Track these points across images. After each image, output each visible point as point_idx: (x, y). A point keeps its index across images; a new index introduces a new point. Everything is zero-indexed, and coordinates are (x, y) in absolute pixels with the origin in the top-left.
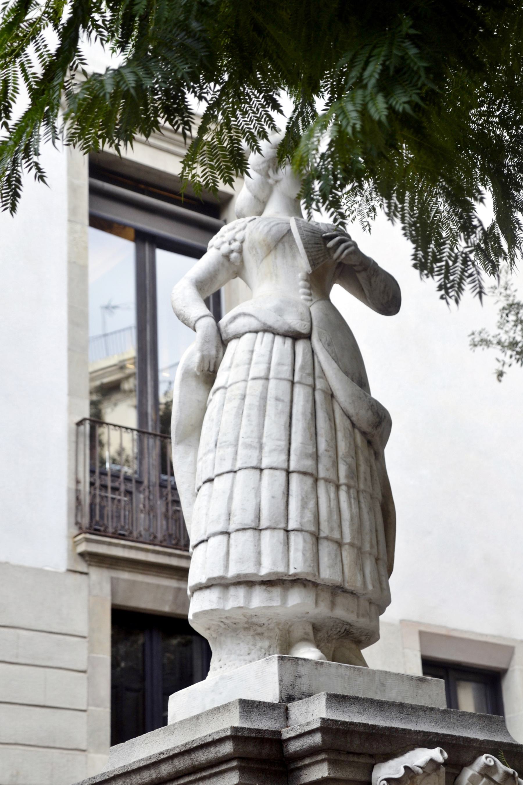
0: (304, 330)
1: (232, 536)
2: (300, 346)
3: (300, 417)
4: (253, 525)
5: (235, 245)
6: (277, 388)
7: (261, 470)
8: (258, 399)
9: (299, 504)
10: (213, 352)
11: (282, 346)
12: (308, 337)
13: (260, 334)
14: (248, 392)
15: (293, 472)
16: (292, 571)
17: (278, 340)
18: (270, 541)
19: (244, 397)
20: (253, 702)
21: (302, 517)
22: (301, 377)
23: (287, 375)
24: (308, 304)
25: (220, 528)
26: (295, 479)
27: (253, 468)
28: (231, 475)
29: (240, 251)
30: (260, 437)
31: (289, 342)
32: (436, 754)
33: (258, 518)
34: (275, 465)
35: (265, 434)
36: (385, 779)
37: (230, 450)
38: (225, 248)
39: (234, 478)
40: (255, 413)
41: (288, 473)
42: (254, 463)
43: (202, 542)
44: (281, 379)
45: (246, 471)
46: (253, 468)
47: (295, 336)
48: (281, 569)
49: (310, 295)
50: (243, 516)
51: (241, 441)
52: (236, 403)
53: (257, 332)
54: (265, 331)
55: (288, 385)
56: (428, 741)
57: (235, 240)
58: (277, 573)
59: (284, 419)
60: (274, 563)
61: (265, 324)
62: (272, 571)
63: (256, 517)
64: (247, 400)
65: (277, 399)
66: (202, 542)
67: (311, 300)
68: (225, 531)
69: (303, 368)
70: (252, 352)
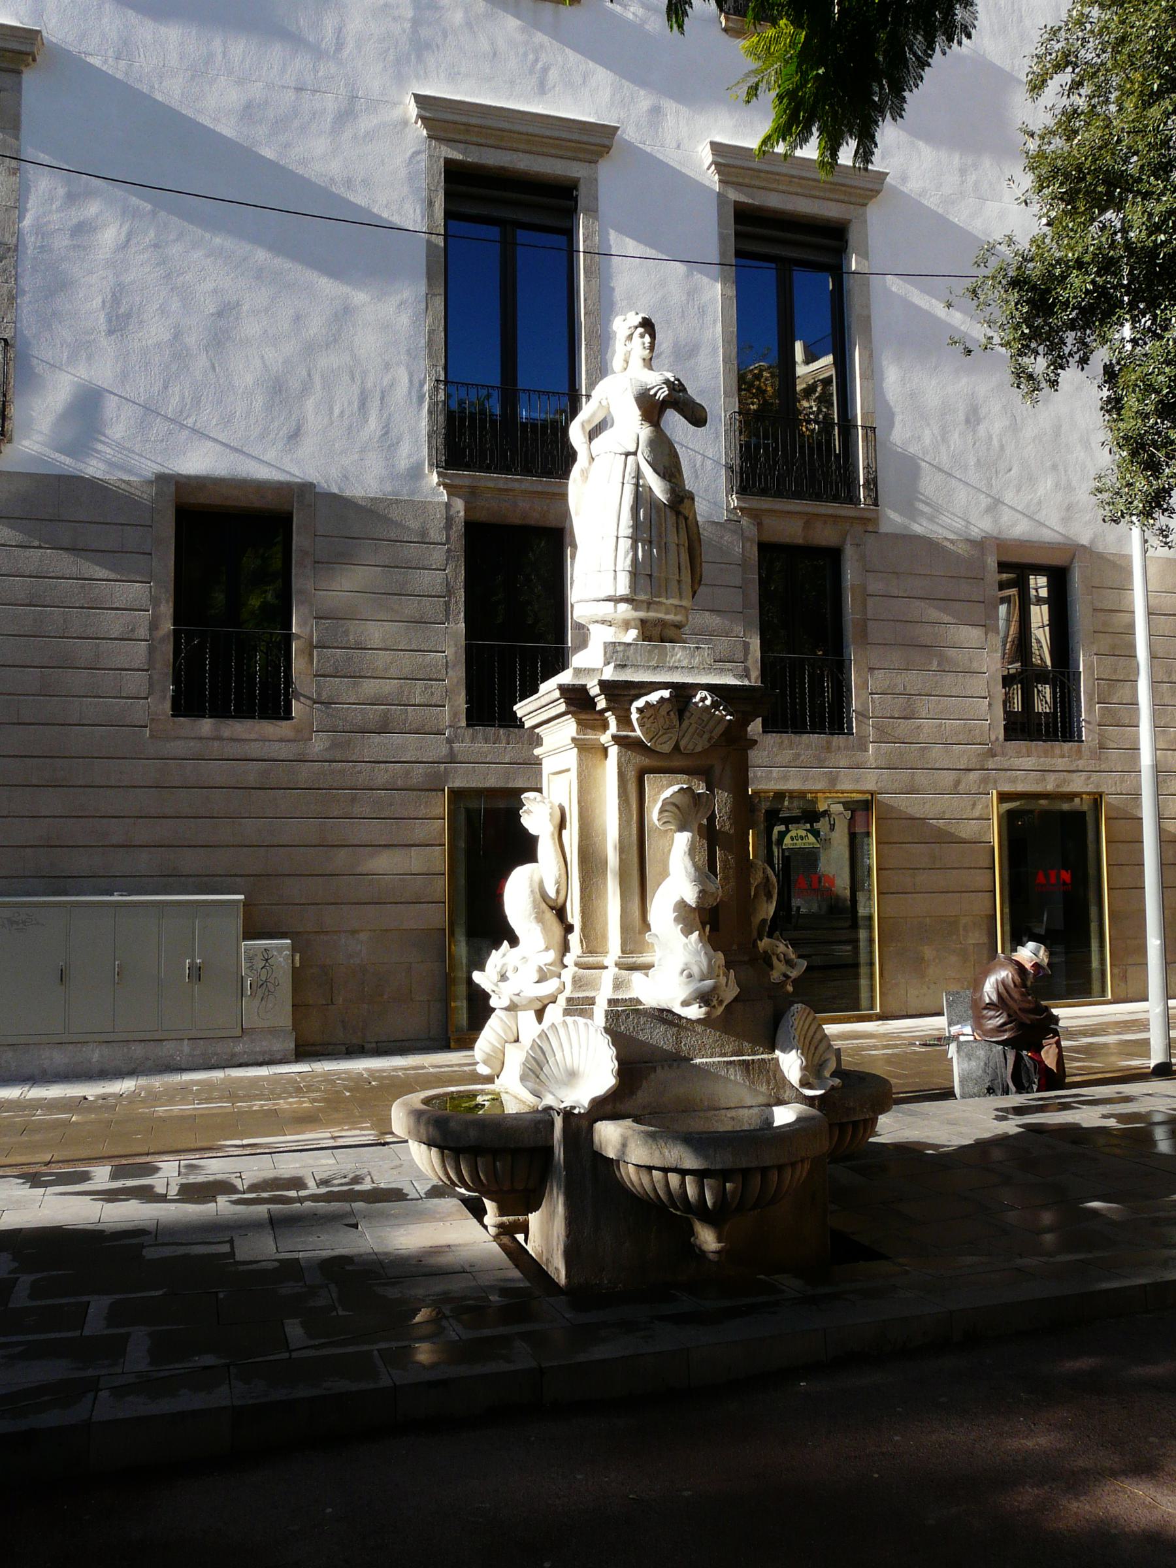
2: (631, 458)
12: (635, 454)
32: (666, 693)
47: (627, 454)
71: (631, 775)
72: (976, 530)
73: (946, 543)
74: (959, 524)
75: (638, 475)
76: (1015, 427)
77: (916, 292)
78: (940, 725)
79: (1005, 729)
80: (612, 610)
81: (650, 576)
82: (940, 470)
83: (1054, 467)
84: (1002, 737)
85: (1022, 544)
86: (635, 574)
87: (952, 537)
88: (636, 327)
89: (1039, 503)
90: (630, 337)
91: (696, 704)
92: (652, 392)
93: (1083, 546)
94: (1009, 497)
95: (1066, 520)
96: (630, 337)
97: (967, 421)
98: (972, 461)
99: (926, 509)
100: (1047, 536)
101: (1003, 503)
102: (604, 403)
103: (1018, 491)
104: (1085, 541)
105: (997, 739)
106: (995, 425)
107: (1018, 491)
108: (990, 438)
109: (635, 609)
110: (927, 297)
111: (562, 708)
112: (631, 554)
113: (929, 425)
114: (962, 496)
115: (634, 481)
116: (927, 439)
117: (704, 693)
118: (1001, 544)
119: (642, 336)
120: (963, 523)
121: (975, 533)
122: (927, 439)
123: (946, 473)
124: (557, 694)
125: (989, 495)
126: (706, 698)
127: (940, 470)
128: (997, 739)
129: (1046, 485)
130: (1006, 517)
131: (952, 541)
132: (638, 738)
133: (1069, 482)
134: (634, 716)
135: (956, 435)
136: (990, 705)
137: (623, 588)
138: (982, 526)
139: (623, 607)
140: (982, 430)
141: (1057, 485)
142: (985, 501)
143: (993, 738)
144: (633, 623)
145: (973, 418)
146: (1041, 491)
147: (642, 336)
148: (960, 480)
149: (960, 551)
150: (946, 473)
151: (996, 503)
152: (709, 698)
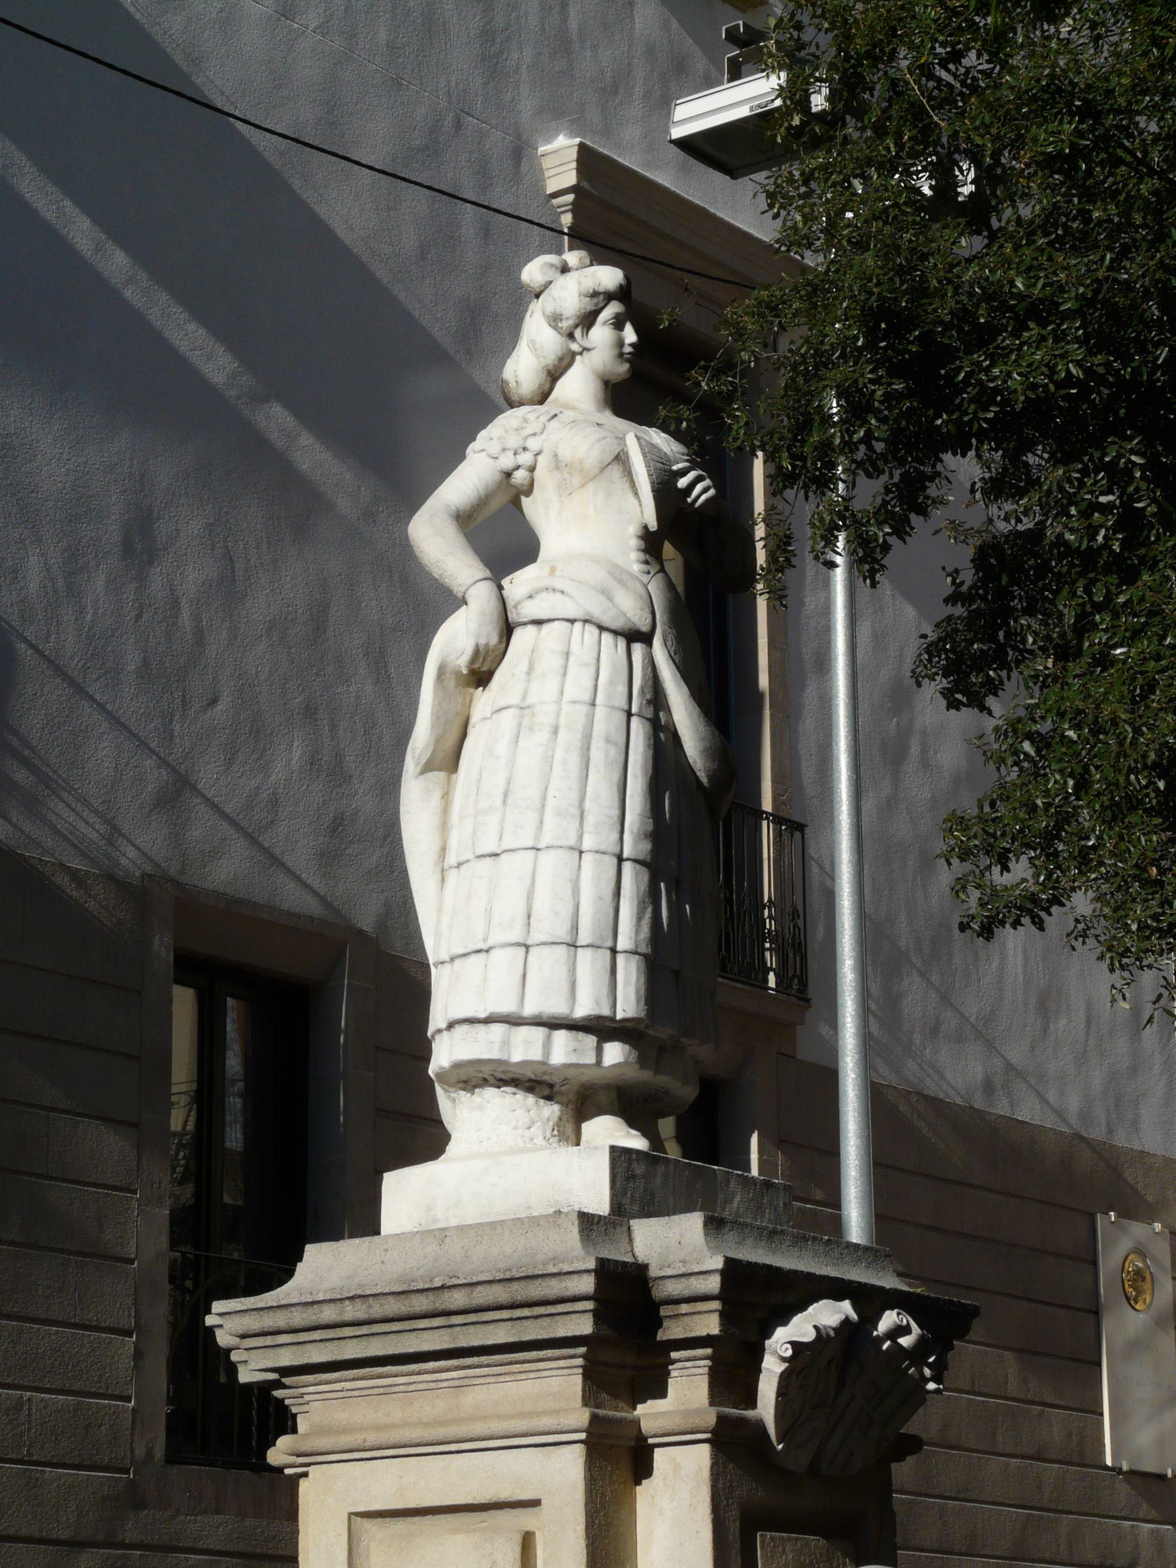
0: (645, 627)
1: (532, 951)
2: (638, 649)
3: (639, 773)
4: (568, 939)
5: (525, 459)
6: (606, 722)
7: (581, 852)
8: (579, 736)
9: (635, 911)
10: (494, 640)
11: (612, 649)
12: (646, 638)
13: (578, 626)
14: (562, 721)
15: (628, 859)
16: (619, 1016)
17: (607, 638)
18: (590, 966)
19: (555, 730)
20: (593, 1215)
21: (637, 932)
22: (640, 708)
23: (622, 702)
24: (645, 578)
25: (516, 935)
26: (627, 867)
27: (571, 848)
28: (533, 852)
29: (532, 469)
30: (582, 800)
31: (622, 643)
33: (575, 928)
34: (603, 848)
35: (588, 795)
36: (789, 1342)
37: (533, 816)
38: (507, 462)
39: (536, 859)
40: (574, 760)
41: (620, 859)
42: (572, 841)
43: (479, 951)
44: (613, 707)
45: (560, 851)
46: (571, 848)
48: (606, 1011)
49: (646, 562)
50: (550, 922)
51: (550, 803)
52: (542, 736)
53: (572, 621)
54: (586, 621)
55: (624, 717)
56: (836, 1289)
57: (525, 449)
58: (599, 1018)
59: (616, 775)
60: (597, 1003)
61: (588, 614)
62: (593, 1013)
63: (572, 927)
64: (562, 733)
65: (608, 740)
66: (479, 951)
67: (649, 573)
68: (522, 941)
69: (642, 691)
70: (567, 654)
71: (734, 1528)
72: (131, 853)
73: (63, 880)
74: (91, 831)
75: (657, 698)
76: (228, 589)
77: (29, 169)
78: (18, 1406)
79: (170, 1430)
80: (590, 1059)
81: (677, 973)
82: (59, 671)
83: (310, 712)
84: (159, 1453)
85: (234, 911)
86: (662, 962)
87: (75, 864)
88: (609, 297)
89: (274, 802)
90: (588, 320)
91: (880, 1340)
92: (683, 483)
93: (361, 932)
94: (209, 774)
95: (328, 858)
96: (588, 320)
97: (127, 549)
98: (132, 661)
99: (22, 776)
100: (293, 898)
101: (194, 788)
102: (520, 476)
103: (230, 762)
104: (366, 922)
105: (150, 1454)
106: (188, 571)
107: (230, 762)
108: (175, 603)
109: (642, 1062)
110: (51, 188)
111: (584, 1326)
112: (650, 909)
113: (39, 540)
114: (103, 751)
115: (649, 713)
116: (33, 584)
117: (906, 1319)
118: (189, 906)
119: (618, 324)
120: (102, 828)
121: (129, 859)
122: (33, 584)
123: (72, 683)
124: (587, 1284)
125: (163, 762)
126: (906, 1330)
127: (59, 671)
128: (150, 1454)
129: (289, 756)
130: (201, 827)
131: (74, 874)
132: (760, 1425)
133: (339, 757)
134: (772, 1368)
135: (100, 581)
136: (138, 1354)
137: (628, 1006)
138: (144, 845)
139: (615, 1053)
140: (157, 575)
141: (313, 759)
142: (155, 778)
143: (140, 1452)
144: (603, 1098)
145: (140, 545)
146: (278, 773)
147: (618, 324)
148: (102, 707)
149: (92, 905)
150: (72, 683)
151: (178, 790)
152: (916, 1330)
